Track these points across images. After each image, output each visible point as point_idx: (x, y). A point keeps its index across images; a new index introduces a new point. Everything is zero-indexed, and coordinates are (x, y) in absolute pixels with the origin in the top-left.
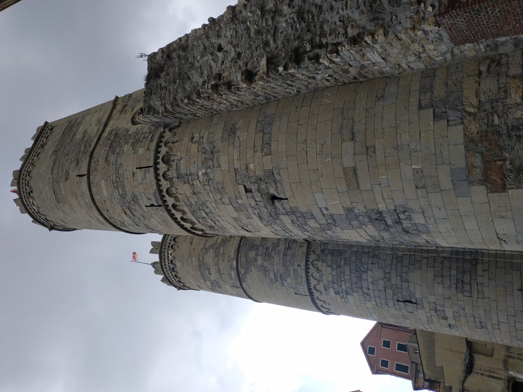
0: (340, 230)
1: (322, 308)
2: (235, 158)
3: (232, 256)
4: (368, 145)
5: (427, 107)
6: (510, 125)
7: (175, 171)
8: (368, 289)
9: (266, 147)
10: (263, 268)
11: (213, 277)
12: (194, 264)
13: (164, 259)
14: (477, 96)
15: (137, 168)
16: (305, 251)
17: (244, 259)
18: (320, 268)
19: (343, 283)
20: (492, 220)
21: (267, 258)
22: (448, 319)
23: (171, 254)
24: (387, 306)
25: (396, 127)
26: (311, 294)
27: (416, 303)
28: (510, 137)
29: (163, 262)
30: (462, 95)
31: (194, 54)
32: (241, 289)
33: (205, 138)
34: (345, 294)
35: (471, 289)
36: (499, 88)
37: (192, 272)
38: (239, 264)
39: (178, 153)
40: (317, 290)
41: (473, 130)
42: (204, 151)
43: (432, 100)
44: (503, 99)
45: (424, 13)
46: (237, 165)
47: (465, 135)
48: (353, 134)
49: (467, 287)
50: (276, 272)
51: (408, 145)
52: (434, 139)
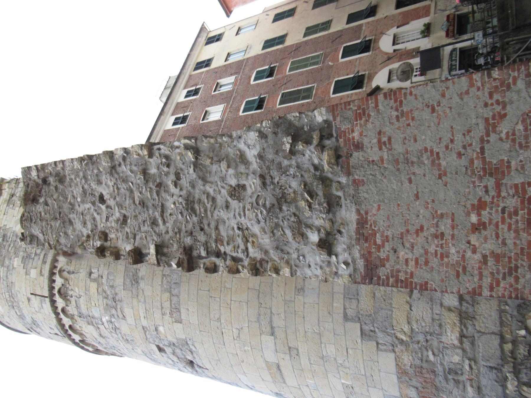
2: (142, 315)
4: (290, 345)
5: (352, 320)
6: (447, 367)
7: (76, 309)
9: (175, 311)
14: (409, 323)
15: (32, 294)
25: (320, 334)
28: (446, 379)
30: (392, 314)
31: (73, 192)
33: (105, 277)
36: (433, 320)
39: (76, 290)
41: (406, 363)
42: (104, 294)
43: (359, 312)
44: (438, 335)
45: (337, 268)
46: (145, 323)
47: (397, 365)
48: (272, 328)
51: (335, 359)
52: (363, 360)
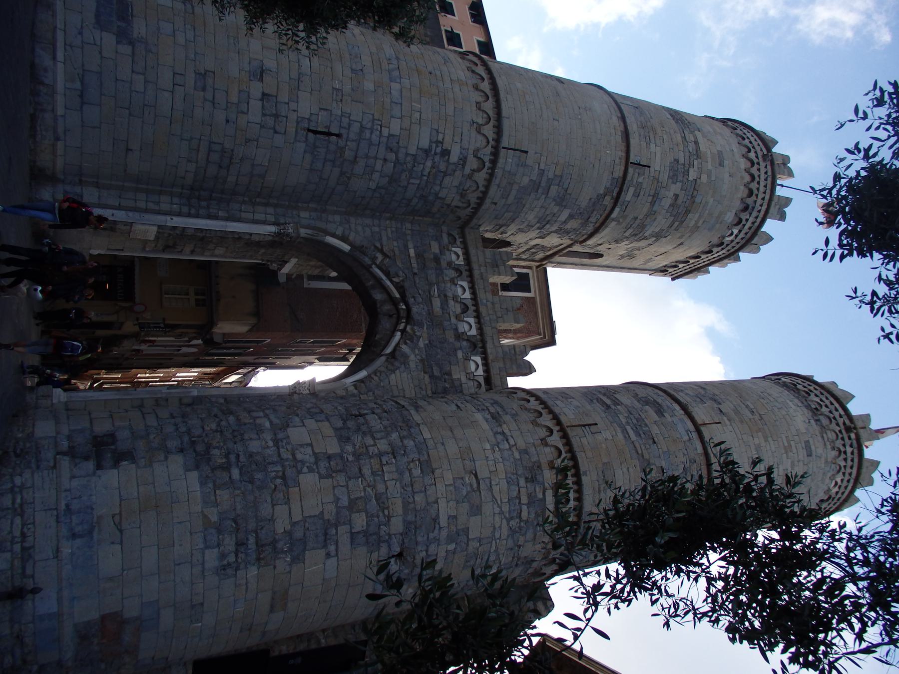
0: (325, 512)
1: (491, 113)
3: (614, 224)
8: (385, 160)
10: (564, 204)
11: (675, 188)
12: (697, 215)
13: (750, 228)
16: (475, 221)
17: (593, 219)
18: (458, 197)
19: (427, 170)
20: (123, 571)
21: (548, 218)
22: (259, 95)
23: (732, 234)
24: (364, 123)
26: (495, 154)
27: (309, 130)
29: (756, 224)
32: (632, 159)
34: (430, 150)
35: (209, 154)
37: (711, 200)
38: (607, 212)
40: (479, 158)
49: (215, 157)
50: (543, 196)
